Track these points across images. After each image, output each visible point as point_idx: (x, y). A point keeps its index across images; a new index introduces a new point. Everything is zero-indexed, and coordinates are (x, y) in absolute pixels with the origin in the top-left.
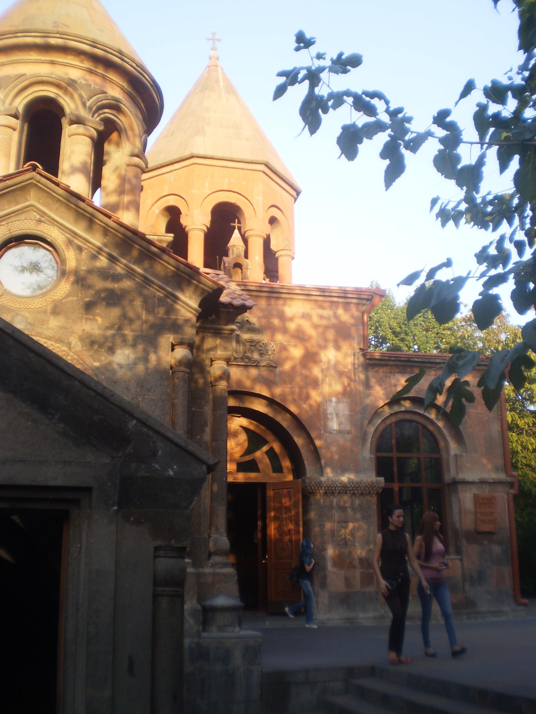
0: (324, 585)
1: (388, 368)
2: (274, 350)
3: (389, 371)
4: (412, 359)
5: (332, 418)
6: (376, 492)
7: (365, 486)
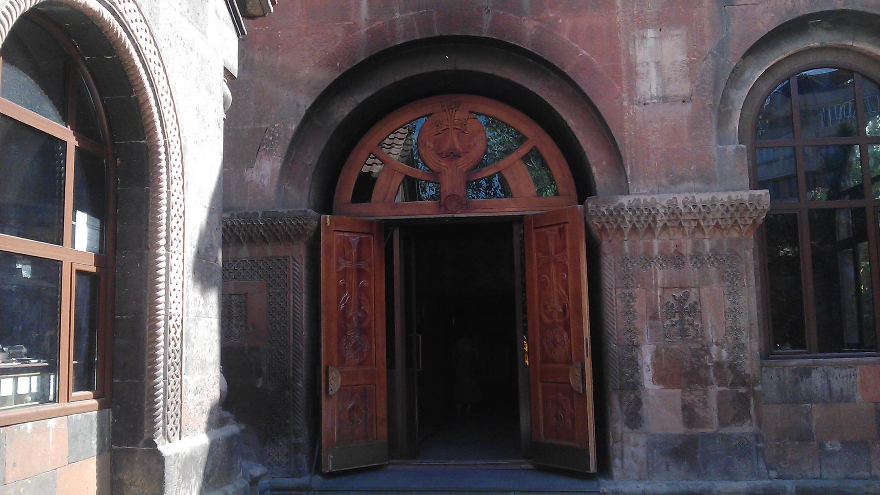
0: (634, 420)
5: (648, 73)
6: (750, 222)
7: (722, 209)
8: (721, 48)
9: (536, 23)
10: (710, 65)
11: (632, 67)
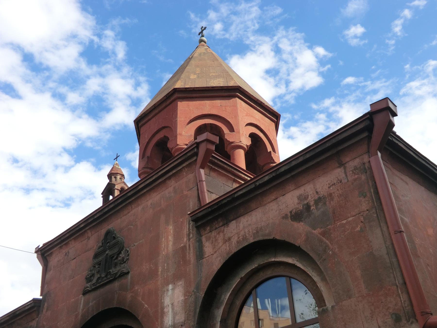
1: (219, 220)
2: (128, 255)
3: (221, 224)
4: (236, 195)
5: (168, 312)
8: (198, 288)
9: (131, 294)
10: (193, 299)
11: (163, 308)
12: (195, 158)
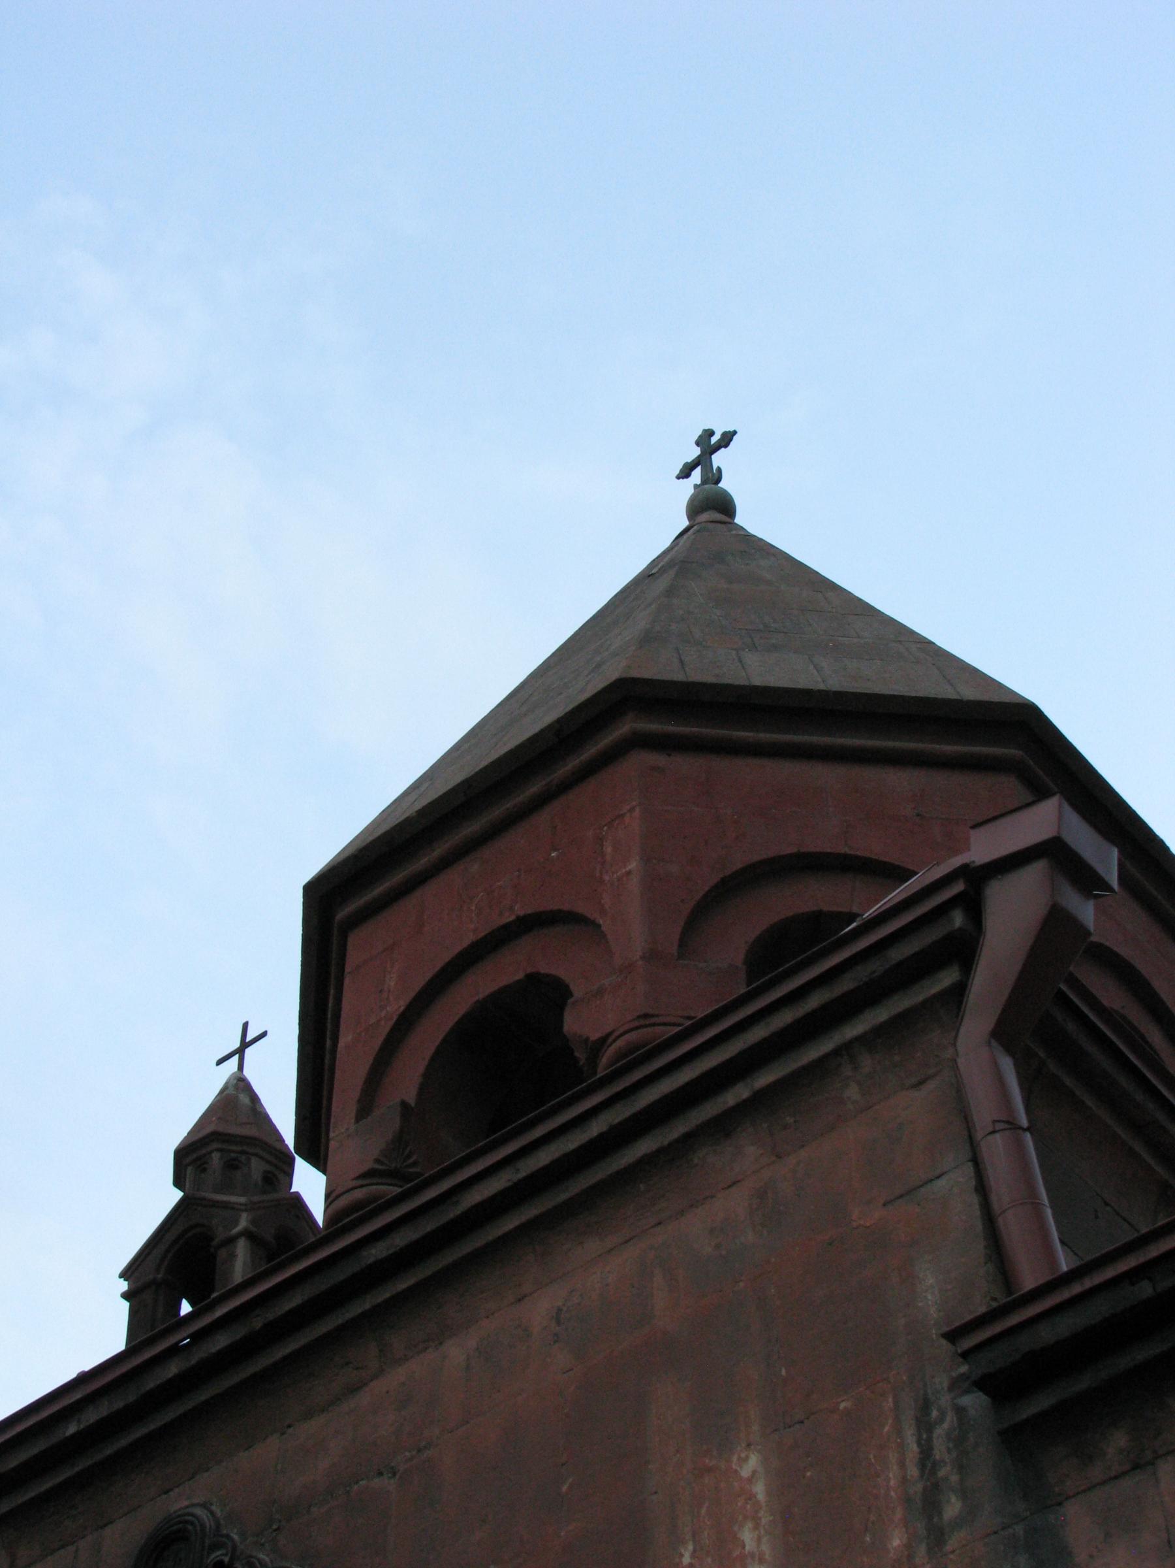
12: (947, 978)
